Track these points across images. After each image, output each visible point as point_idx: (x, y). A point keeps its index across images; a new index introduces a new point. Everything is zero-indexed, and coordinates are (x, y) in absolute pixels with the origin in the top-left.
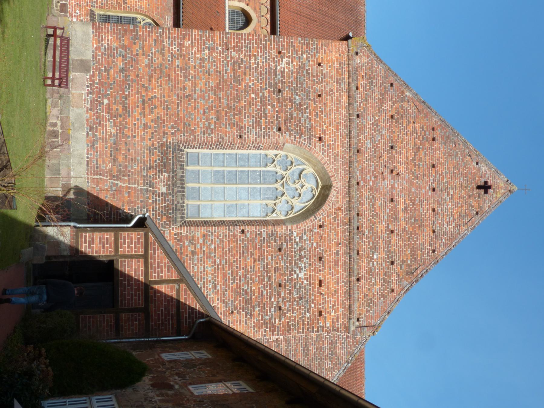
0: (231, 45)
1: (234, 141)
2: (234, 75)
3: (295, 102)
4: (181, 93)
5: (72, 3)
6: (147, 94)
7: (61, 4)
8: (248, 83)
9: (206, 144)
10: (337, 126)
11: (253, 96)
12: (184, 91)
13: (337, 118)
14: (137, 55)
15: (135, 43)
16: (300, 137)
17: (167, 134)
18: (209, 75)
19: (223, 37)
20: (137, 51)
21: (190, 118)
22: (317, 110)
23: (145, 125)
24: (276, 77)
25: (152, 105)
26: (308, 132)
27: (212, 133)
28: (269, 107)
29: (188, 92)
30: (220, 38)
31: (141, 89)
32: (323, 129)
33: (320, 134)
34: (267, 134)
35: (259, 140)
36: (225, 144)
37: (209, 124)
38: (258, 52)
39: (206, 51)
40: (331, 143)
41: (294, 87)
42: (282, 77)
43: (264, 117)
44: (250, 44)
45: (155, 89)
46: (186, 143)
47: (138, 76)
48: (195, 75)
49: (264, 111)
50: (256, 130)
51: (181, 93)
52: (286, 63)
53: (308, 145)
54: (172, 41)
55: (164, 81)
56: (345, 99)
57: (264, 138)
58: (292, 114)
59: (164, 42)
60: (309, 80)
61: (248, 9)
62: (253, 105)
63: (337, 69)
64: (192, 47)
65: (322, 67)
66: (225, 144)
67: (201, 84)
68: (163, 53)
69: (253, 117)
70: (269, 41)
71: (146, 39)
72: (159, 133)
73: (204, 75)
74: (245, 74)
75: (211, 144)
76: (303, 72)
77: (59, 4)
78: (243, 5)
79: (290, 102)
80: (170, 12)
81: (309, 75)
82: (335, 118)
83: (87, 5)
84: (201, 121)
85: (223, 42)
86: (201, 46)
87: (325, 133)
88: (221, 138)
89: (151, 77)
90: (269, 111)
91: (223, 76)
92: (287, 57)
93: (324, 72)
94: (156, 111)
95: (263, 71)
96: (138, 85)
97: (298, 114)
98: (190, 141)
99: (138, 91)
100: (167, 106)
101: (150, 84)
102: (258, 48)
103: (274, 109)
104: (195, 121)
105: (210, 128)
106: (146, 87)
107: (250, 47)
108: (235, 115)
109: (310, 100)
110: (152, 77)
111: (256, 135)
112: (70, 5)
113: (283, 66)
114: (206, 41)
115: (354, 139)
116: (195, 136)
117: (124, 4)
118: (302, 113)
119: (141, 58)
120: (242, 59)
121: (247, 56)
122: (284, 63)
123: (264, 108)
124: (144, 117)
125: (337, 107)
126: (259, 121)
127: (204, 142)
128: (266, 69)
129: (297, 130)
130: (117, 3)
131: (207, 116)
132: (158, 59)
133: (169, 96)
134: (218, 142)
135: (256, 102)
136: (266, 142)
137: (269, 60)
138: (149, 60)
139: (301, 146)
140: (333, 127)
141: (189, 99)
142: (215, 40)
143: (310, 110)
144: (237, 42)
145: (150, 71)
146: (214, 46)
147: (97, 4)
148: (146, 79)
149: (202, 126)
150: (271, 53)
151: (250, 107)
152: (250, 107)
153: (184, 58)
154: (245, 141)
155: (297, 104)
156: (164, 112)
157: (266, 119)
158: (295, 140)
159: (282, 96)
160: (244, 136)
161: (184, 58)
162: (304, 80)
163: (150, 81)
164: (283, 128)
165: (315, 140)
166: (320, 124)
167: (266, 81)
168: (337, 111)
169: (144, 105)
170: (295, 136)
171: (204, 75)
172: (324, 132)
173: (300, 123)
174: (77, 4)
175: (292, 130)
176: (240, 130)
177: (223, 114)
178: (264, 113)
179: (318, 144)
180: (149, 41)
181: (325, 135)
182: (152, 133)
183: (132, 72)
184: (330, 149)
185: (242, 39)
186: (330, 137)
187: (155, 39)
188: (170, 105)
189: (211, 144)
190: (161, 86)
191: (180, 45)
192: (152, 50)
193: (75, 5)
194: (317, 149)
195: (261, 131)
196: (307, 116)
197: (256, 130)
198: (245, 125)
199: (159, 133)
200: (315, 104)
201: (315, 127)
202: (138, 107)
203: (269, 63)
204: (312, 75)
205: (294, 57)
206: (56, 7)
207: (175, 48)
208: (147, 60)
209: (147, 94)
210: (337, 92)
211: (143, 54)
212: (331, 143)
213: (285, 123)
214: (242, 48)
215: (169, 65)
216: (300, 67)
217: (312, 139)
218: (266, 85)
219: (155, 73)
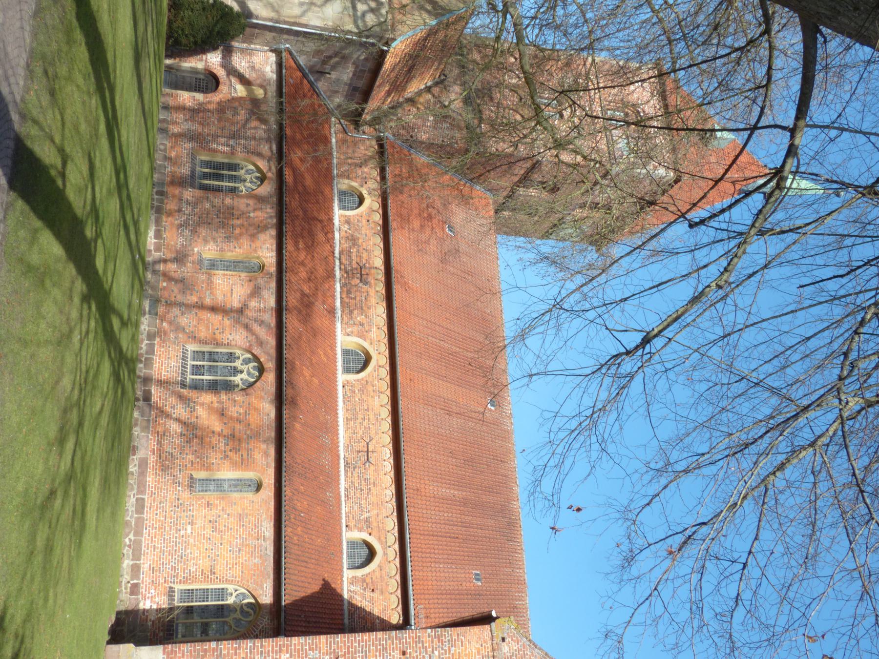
5: (146, 581)
7: (132, 584)
19: (331, 642)
30: (327, 644)
61: (370, 539)
77: (129, 585)
78: (364, 536)
80: (269, 578)
83: (165, 582)
112: (143, 583)
114: (310, 650)
117: (211, 575)
130: (202, 575)
142: (320, 648)
147: (177, 578)
174: (153, 581)
193: (149, 584)
206: (126, 589)
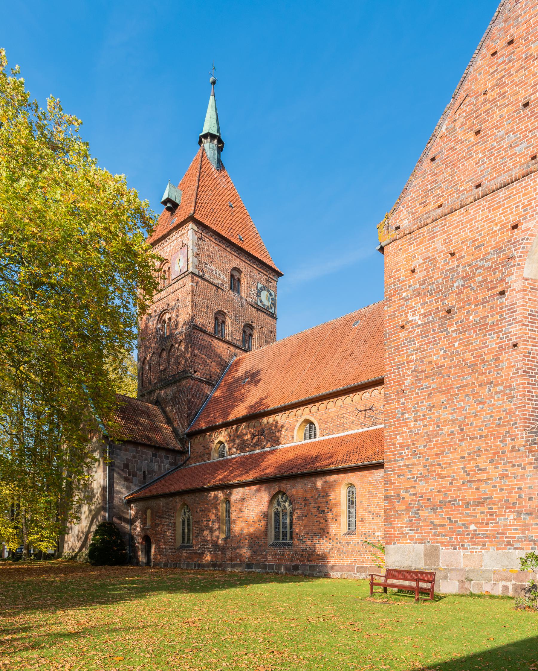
0: (398, 388)
1: (523, 352)
2: (432, 376)
3: (462, 285)
4: (457, 438)
6: (461, 479)
8: (441, 356)
9: (528, 392)
10: (493, 210)
11: (456, 345)
12: (455, 434)
13: (482, 215)
14: (415, 494)
15: (403, 498)
16: (513, 258)
17: (514, 447)
18: (433, 407)
20: (411, 495)
21: (489, 421)
22: (472, 249)
23: (502, 477)
24: (431, 321)
25: (474, 471)
26: (504, 250)
27: (510, 386)
28: (471, 318)
29: (456, 429)
31: (455, 487)
32: (499, 230)
33: (507, 231)
34: (509, 310)
35: (519, 318)
36: (528, 364)
37: (497, 393)
38: (403, 354)
39: (407, 416)
40: (521, 207)
41: (443, 293)
42: (430, 315)
43: (485, 321)
44: (395, 366)
45: (454, 469)
46: (529, 419)
47: (439, 492)
48: (435, 424)
49: (476, 324)
50: (505, 326)
51: (457, 438)
52: (414, 315)
53: (525, 241)
54: (398, 457)
55: (443, 460)
56: (455, 217)
57: (516, 311)
58: (480, 282)
59: (400, 466)
60: (433, 277)
62: (468, 341)
63: (417, 245)
64: (403, 433)
65: (416, 266)
66: (528, 364)
67: (446, 415)
68: (412, 465)
69: (485, 335)
70: (390, 345)
71: (397, 486)
72: (513, 458)
73: (434, 413)
74: (430, 363)
75: (529, 384)
76: (423, 289)
79: (463, 292)
81: (426, 280)
82: (483, 219)
84: (494, 405)
85: (395, 399)
86: (401, 423)
87: (505, 224)
88: (518, 373)
89: (440, 476)
90: (476, 317)
91: (434, 389)
92: (407, 316)
93: (422, 261)
94: (482, 465)
95: (424, 340)
96: (450, 491)
97: (480, 274)
98: (526, 415)
99: (458, 490)
100: (475, 452)
101: (449, 477)
102: (399, 355)
103: (474, 310)
104: (494, 413)
105: (504, 391)
106: (452, 480)
107: (399, 365)
108: (484, 361)
109: (458, 266)
110: (439, 474)
111: (512, 324)
113: (417, 318)
115: (513, 173)
116: (516, 408)
118: (476, 269)
119: (418, 490)
120: (413, 371)
121: (409, 365)
122: (414, 318)
123: (473, 325)
124: (491, 479)
125: (466, 222)
126: (490, 327)
127: (524, 395)
128: (422, 338)
129: (502, 267)
131: (487, 399)
132: (418, 471)
133: (463, 451)
134: (523, 375)
135: (465, 339)
136: (523, 305)
137: (411, 338)
138: (421, 481)
139: (527, 252)
140: (495, 216)
141: (464, 425)
143: (473, 260)
144: (394, 382)
145: (432, 477)
146: (400, 407)
148: (442, 481)
149: (500, 402)
150: (404, 337)
151: (471, 344)
152: (471, 344)
153: (416, 441)
154: (522, 337)
155: (465, 281)
156: (484, 455)
157: (488, 316)
158: (518, 265)
159: (454, 306)
160: (514, 340)
161: (416, 441)
162: (434, 283)
163: (444, 477)
164: (500, 289)
165: (518, 234)
166: (492, 237)
167: (437, 333)
168: (472, 220)
169: (474, 481)
170: (511, 267)
171: (434, 413)
172: (503, 227)
173: (491, 267)
175: (503, 274)
176: (505, 349)
177: (483, 377)
178: (480, 323)
179: (523, 227)
180: (400, 482)
181: (509, 222)
182: (514, 466)
183: (434, 499)
184: (531, 204)
185: (391, 377)
186: (512, 213)
187: (398, 476)
188: (474, 449)
189: (529, 384)
190: (450, 463)
191: (402, 446)
192: (409, 479)
194: (531, 224)
195: (505, 318)
196: (482, 260)
197: (505, 326)
198: (497, 344)
199: (513, 458)
200: (464, 256)
201: (497, 243)
202: (477, 488)
203: (414, 337)
204: (426, 276)
205: (406, 307)
207: (405, 453)
208: (420, 483)
209: (461, 479)
210: (445, 232)
211: (414, 487)
212: (521, 207)
213: (492, 289)
214: (400, 374)
215: (424, 456)
216: (418, 296)
217: (516, 238)
218: (442, 332)
219: (435, 471)
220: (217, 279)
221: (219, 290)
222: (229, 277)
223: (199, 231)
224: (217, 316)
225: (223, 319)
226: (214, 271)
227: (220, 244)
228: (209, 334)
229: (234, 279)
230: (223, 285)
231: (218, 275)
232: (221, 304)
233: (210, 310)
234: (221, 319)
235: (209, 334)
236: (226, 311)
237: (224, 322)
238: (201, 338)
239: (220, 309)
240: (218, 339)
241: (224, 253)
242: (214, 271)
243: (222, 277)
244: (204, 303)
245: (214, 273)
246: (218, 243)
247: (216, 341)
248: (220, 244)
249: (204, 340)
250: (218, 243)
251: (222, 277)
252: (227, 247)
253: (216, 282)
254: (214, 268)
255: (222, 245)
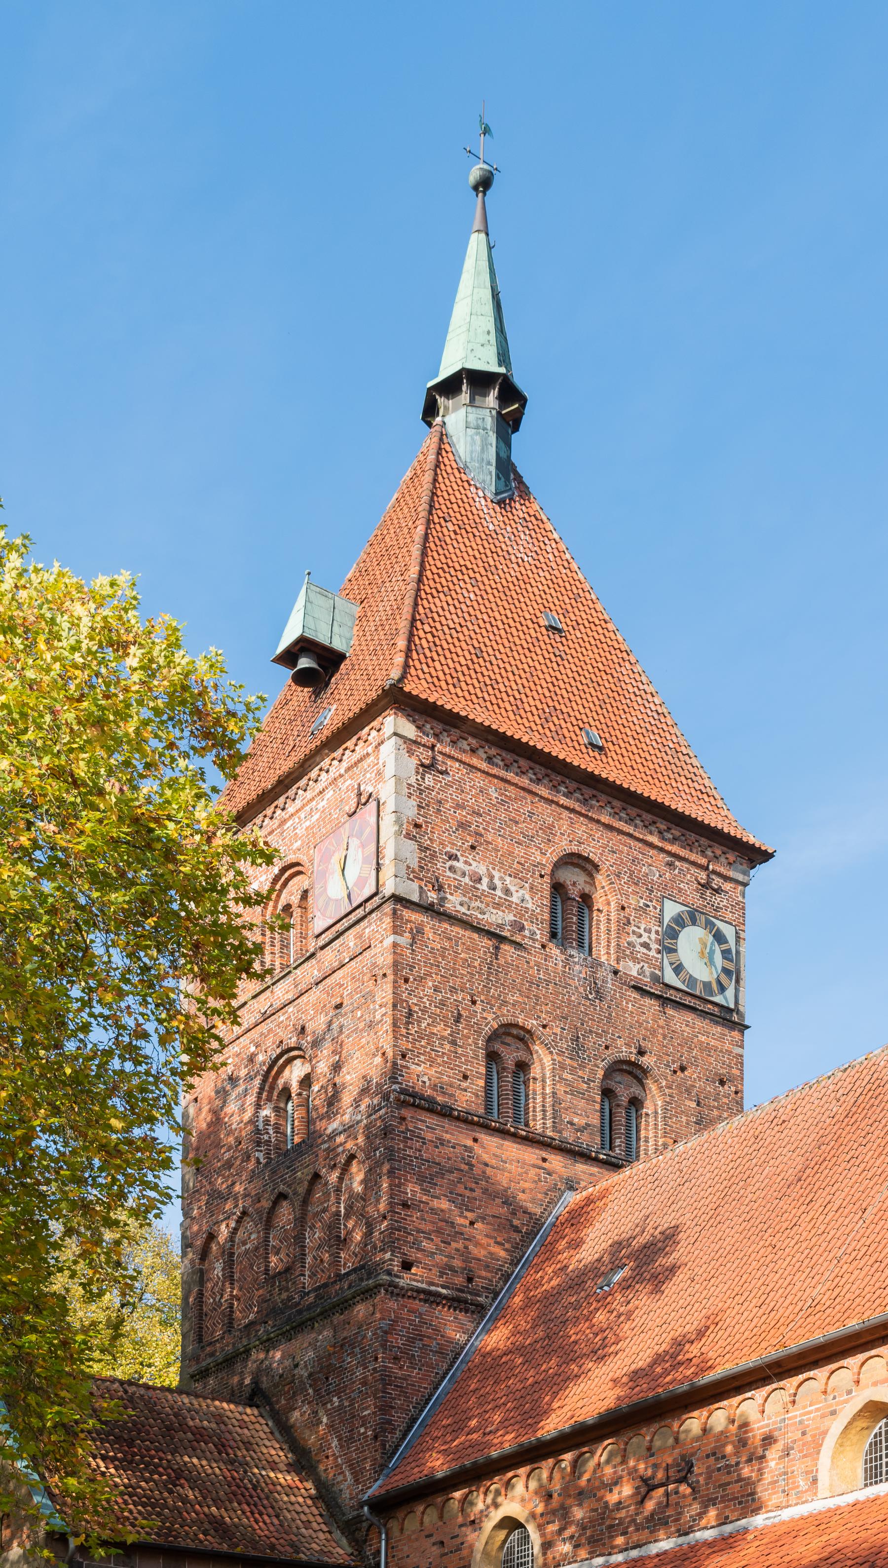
220: (497, 906)
221: (505, 947)
222: (547, 893)
223: (425, 740)
224: (497, 1046)
225: (521, 1055)
226: (485, 881)
227: (510, 776)
228: (465, 1120)
229: (566, 899)
230: (522, 928)
231: (499, 893)
232: (511, 999)
233: (469, 1026)
234: (510, 1055)
235: (465, 1120)
236: (531, 1023)
237: (522, 1067)
238: (429, 1136)
239: (509, 1019)
240: (503, 1133)
241: (526, 805)
242: (485, 881)
243: (515, 899)
244: (443, 1003)
245: (484, 886)
246: (502, 773)
247: (490, 1142)
248: (510, 776)
249: (442, 1142)
250: (502, 773)
251: (515, 899)
252: (538, 781)
253: (494, 918)
254: (482, 869)
255: (516, 780)
